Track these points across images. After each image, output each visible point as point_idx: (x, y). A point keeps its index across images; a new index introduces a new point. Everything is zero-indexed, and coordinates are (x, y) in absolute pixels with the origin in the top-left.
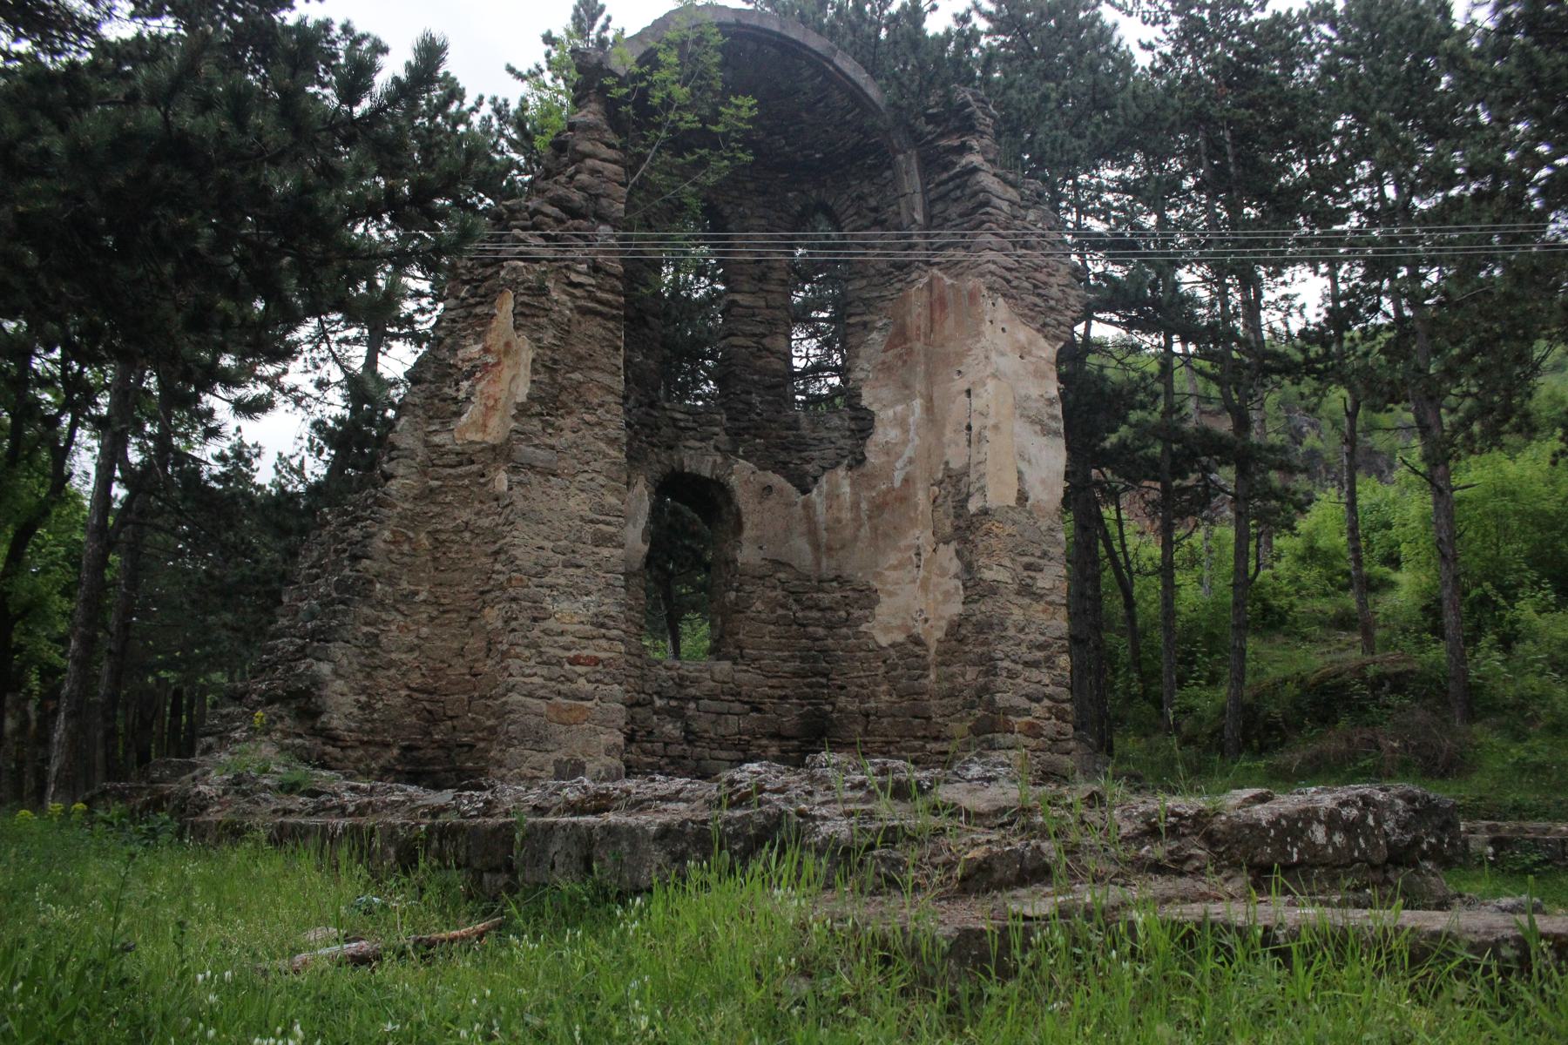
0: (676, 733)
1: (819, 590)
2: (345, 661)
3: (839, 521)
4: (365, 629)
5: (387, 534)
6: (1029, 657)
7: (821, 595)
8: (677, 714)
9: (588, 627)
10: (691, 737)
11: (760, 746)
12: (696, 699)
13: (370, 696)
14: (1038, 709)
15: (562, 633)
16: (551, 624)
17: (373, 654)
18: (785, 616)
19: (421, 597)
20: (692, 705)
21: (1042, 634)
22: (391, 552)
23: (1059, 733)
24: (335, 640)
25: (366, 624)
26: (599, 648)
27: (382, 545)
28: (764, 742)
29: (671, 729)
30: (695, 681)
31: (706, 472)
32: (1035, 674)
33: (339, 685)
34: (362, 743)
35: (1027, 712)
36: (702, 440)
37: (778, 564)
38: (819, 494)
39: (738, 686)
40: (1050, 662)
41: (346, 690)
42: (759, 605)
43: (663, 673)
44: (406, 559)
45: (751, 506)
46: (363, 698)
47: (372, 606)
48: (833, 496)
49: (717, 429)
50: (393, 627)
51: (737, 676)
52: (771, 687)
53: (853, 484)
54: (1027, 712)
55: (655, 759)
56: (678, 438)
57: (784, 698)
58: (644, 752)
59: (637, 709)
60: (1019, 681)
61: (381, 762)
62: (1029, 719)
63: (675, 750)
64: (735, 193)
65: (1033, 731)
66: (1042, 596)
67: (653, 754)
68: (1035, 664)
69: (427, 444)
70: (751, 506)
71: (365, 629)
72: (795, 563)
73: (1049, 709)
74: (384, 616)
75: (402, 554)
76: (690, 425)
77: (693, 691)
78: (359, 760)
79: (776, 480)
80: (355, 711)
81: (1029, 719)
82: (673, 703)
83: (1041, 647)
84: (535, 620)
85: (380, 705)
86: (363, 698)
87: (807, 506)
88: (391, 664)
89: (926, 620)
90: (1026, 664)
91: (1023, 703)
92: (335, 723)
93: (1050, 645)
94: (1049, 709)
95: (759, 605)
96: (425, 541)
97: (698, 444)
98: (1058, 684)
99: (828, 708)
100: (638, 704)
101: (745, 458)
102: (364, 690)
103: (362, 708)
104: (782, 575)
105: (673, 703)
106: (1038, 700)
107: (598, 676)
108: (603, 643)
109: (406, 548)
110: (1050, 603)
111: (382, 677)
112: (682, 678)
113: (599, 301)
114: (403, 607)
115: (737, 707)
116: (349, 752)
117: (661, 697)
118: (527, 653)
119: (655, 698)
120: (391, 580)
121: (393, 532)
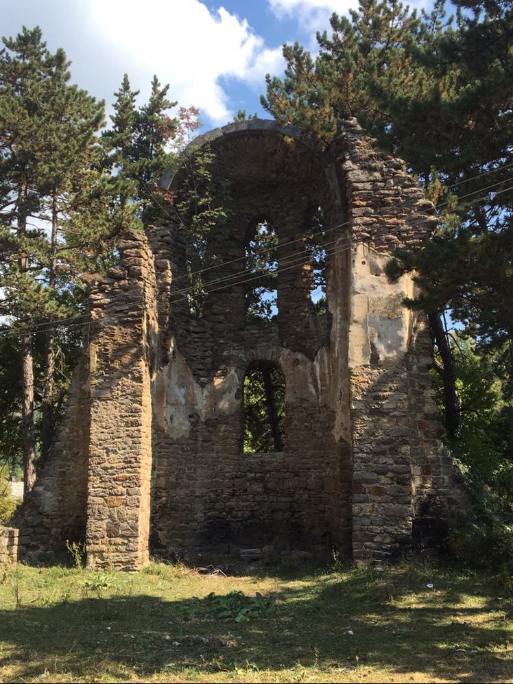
0: (260, 490)
1: (320, 412)
2: (50, 485)
3: (324, 374)
4: (59, 470)
5: (67, 430)
6: (377, 449)
7: (320, 415)
8: (261, 480)
9: (122, 464)
10: (267, 491)
11: (299, 495)
12: (269, 472)
13: (63, 497)
14: (383, 479)
15: (112, 468)
16: (107, 465)
17: (64, 480)
18: (305, 426)
19: (80, 454)
20: (268, 475)
21: (388, 435)
22: (70, 437)
23: (398, 492)
24: (45, 476)
25: (60, 468)
26: (128, 472)
27: (65, 435)
28: (301, 492)
29: (257, 487)
30: (270, 463)
31: (269, 358)
32: (382, 460)
33: (48, 494)
34: (61, 516)
35: (377, 481)
36: (267, 342)
37: (303, 400)
38: (317, 362)
39: (288, 464)
40: (393, 451)
41: (52, 496)
42: (296, 422)
43: (252, 460)
44: (76, 439)
45: (289, 372)
46: (60, 498)
47: (62, 460)
48: (322, 362)
49: (272, 335)
50: (71, 468)
51: (287, 459)
52: (303, 464)
53: (328, 356)
54: (377, 481)
55: (248, 503)
56: (256, 343)
57: (309, 469)
58: (243, 501)
59: (235, 480)
60: (371, 463)
61: (69, 522)
62: (377, 485)
63: (258, 498)
64: (278, 206)
65: (380, 492)
66: (387, 414)
67: (247, 500)
68: (383, 453)
69: (81, 390)
70: (289, 372)
71: (59, 470)
72: (310, 399)
73: (391, 479)
74: (68, 463)
75: (74, 437)
76: (262, 335)
77: (268, 468)
78: (59, 523)
79: (300, 356)
80: (57, 503)
81: (377, 485)
82: (258, 475)
83: (385, 443)
84: (99, 463)
85: (67, 500)
86: (60, 498)
87: (313, 369)
88: (70, 483)
89: (346, 429)
90: (375, 453)
91: (369, 476)
92: (46, 509)
93: (394, 441)
94: (391, 479)
95: (296, 422)
96: (81, 432)
97: (265, 344)
98: (402, 463)
99: (324, 474)
100: (237, 477)
101: (287, 347)
102: (60, 494)
103: (60, 501)
104: (305, 405)
105: (258, 475)
106: (384, 474)
107: (128, 484)
108: (129, 469)
109: (75, 434)
110: (395, 416)
111: (68, 489)
112: (262, 462)
113: (130, 316)
114: (73, 458)
115: (287, 475)
116: (54, 520)
117: (251, 472)
118: (95, 478)
119: (248, 473)
120: (70, 448)
121: (69, 429)
